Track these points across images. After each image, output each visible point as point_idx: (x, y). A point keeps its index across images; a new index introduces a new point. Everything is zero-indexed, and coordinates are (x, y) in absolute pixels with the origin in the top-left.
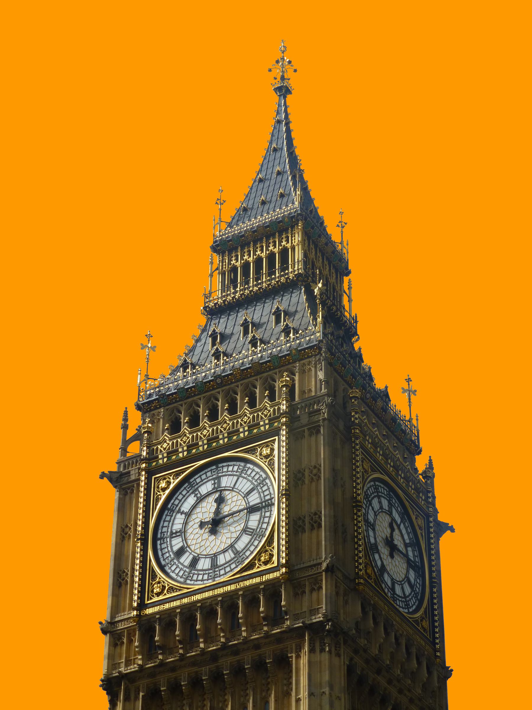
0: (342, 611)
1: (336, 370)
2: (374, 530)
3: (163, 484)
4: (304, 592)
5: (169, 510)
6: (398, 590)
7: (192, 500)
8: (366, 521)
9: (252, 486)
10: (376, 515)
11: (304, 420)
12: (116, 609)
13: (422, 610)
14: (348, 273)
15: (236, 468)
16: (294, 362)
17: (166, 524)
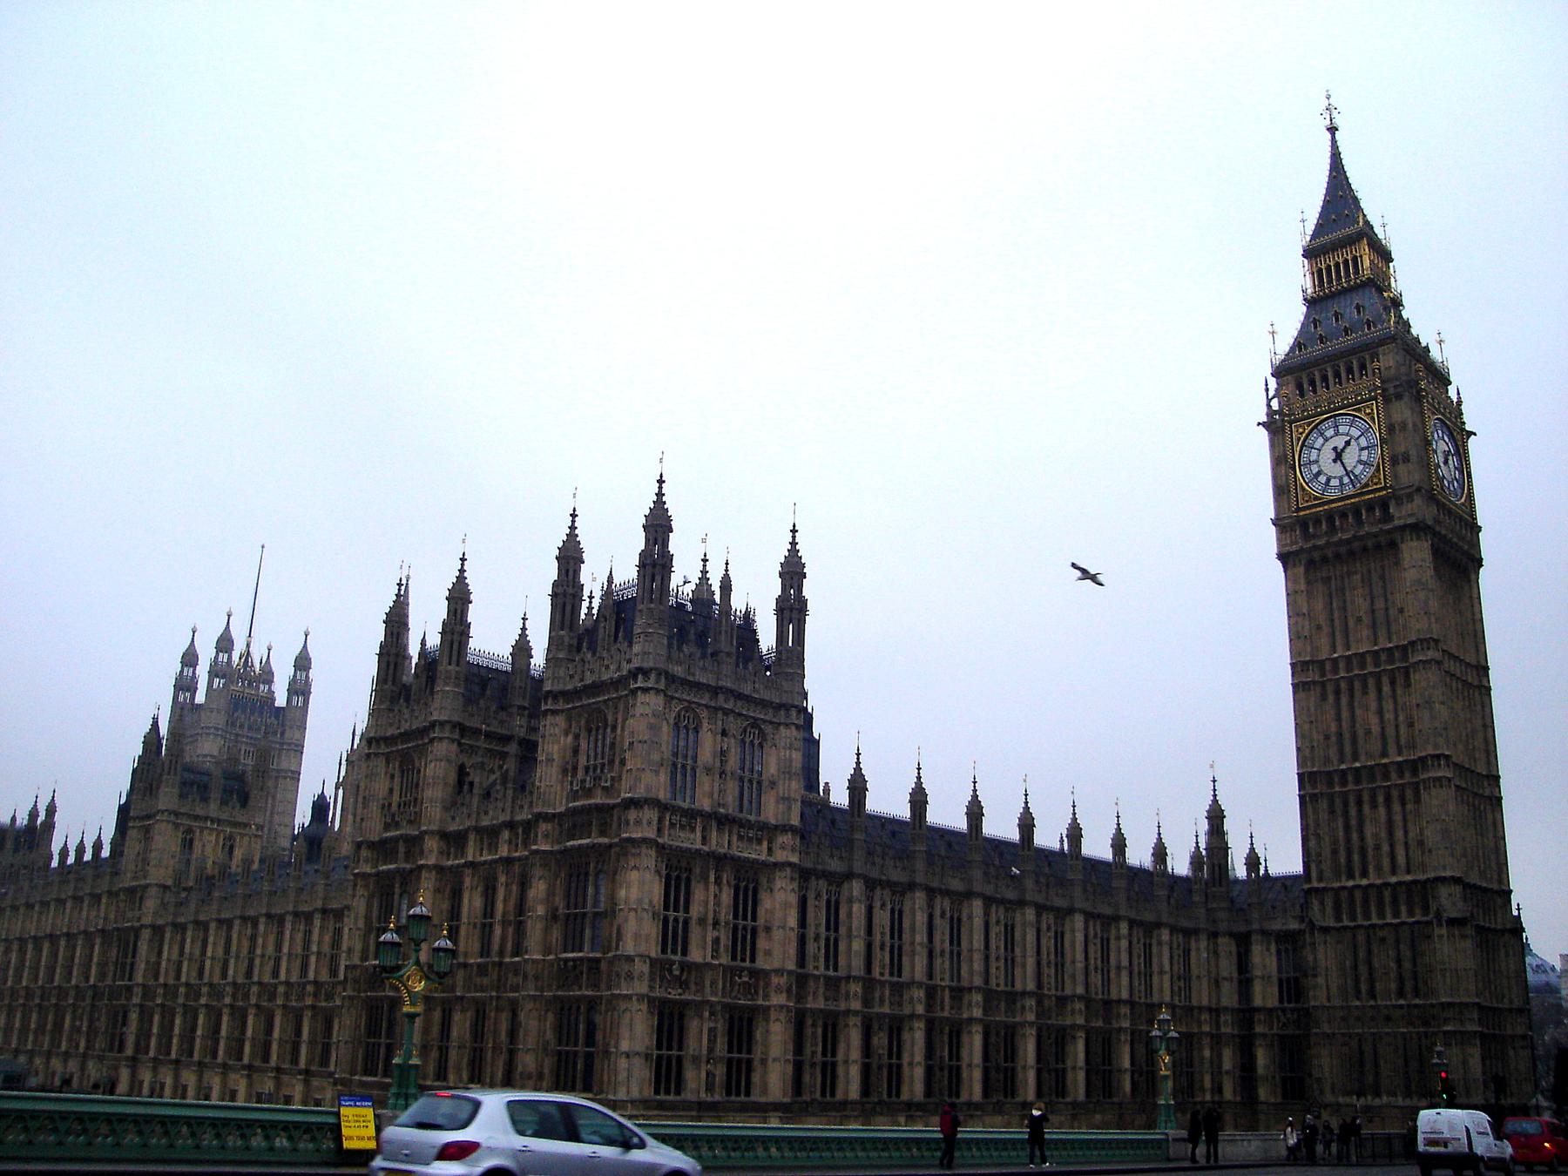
7: (1321, 440)
11: (1392, 391)
12: (1277, 513)
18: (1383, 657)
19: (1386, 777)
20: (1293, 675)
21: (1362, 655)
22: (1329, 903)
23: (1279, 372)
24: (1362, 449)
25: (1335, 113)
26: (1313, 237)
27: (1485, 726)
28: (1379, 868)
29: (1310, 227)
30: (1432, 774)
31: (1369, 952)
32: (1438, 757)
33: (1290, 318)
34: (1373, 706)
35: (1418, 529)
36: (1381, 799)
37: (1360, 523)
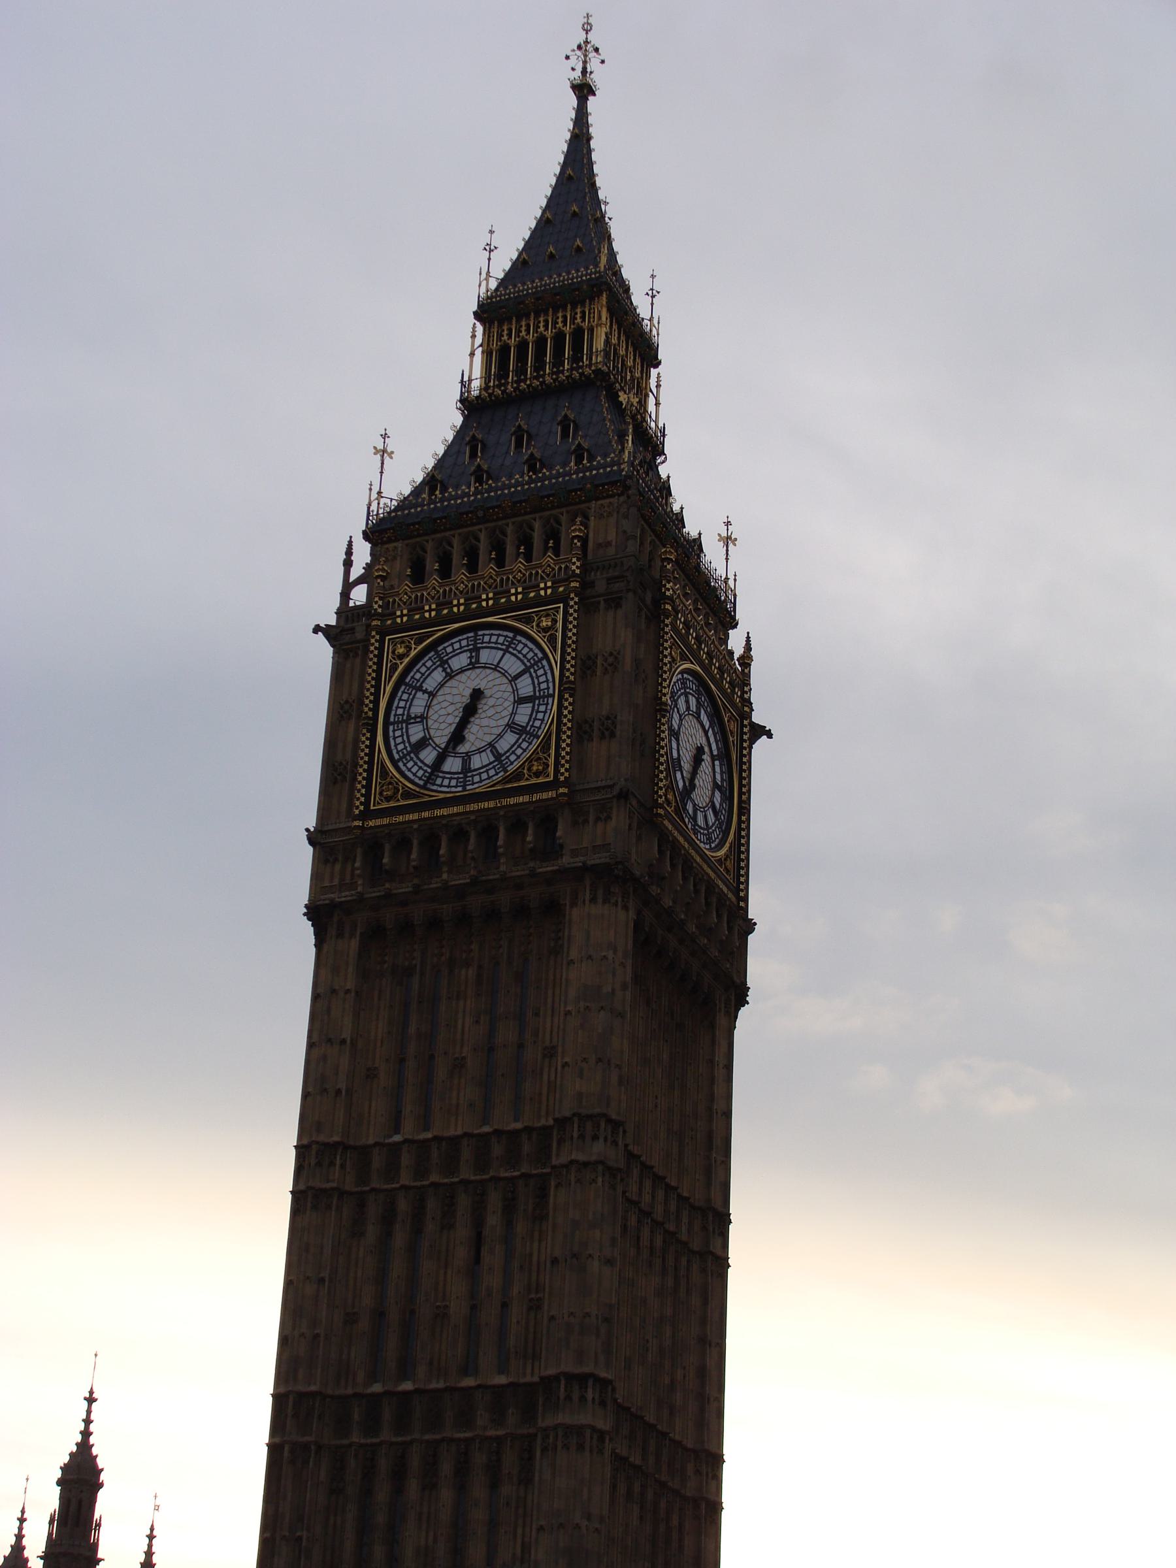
0: (634, 850)
1: (643, 516)
2: (677, 740)
3: (401, 650)
4: (586, 821)
5: (407, 685)
6: (700, 821)
7: (438, 675)
8: (670, 728)
9: (523, 667)
10: (681, 720)
11: (601, 586)
13: (727, 845)
14: (657, 364)
15: (501, 640)
16: (589, 500)
17: (402, 704)
18: (497, 1150)
21: (455, 1141)
24: (521, 701)
25: (594, 64)
26: (503, 283)
27: (703, 1341)
29: (502, 264)
30: (564, 1418)
32: (582, 1379)
33: (425, 431)
34: (461, 1254)
35: (609, 878)
36: (446, 1468)
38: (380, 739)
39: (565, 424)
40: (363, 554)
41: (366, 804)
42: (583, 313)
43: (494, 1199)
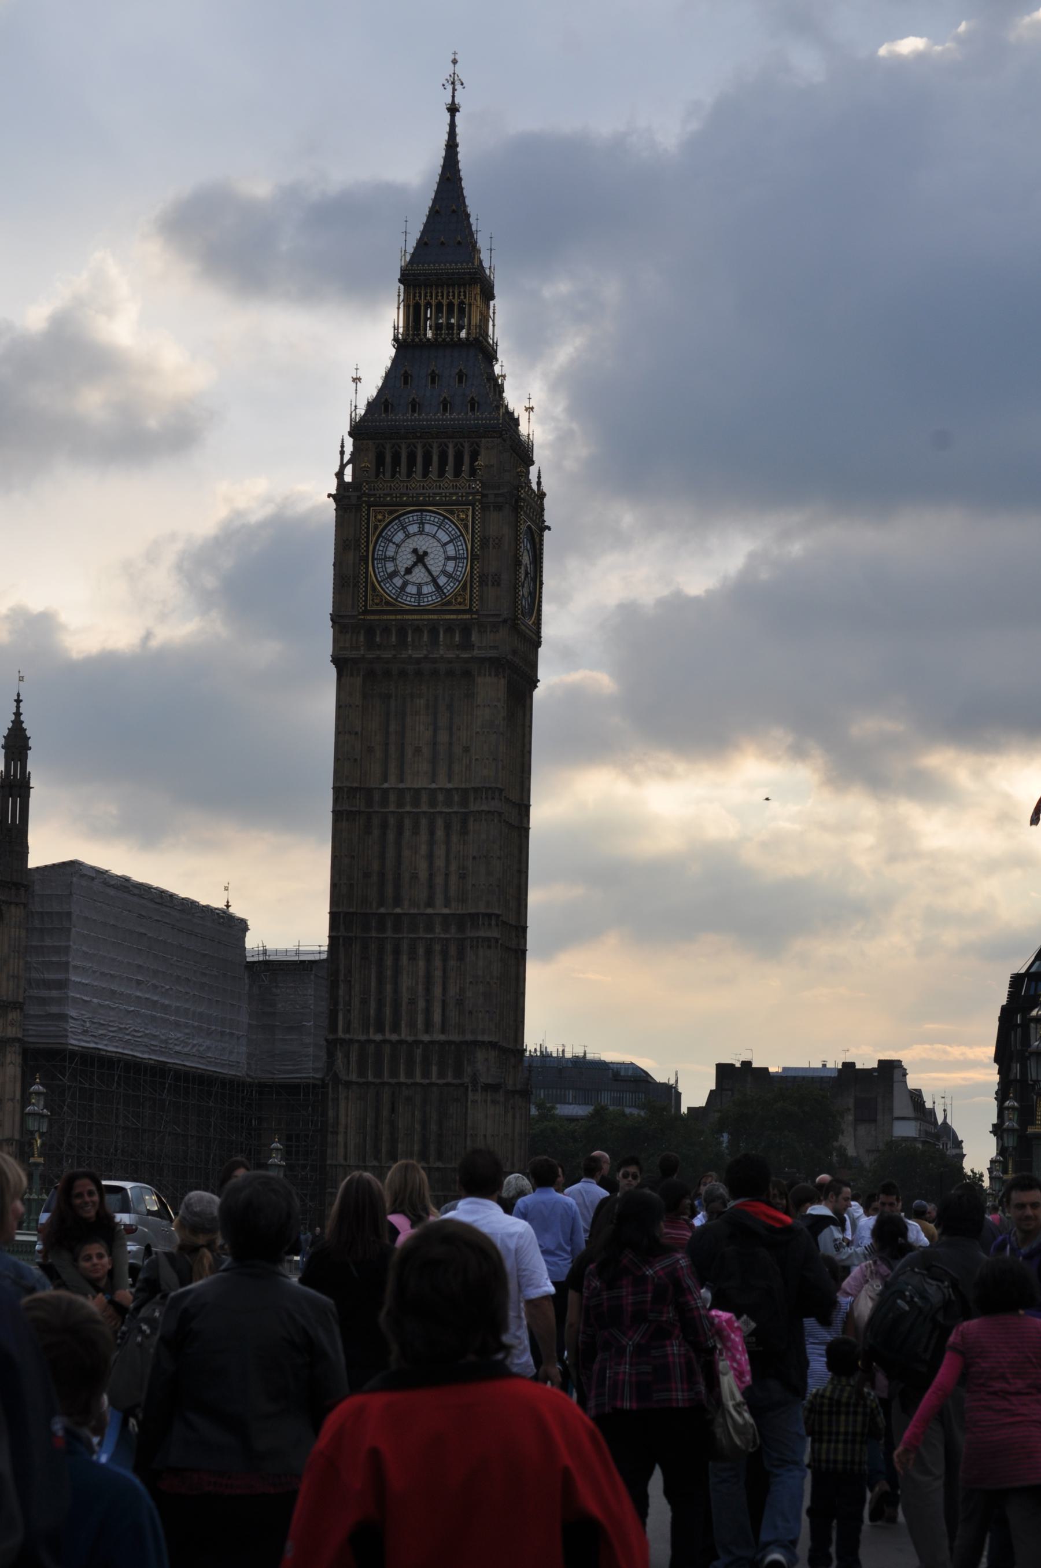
3: (380, 517)
7: (400, 535)
18: (441, 797)
19: (430, 928)
20: (336, 800)
21: (417, 791)
22: (354, 1057)
23: (357, 430)
24: (448, 558)
25: (458, 87)
28: (412, 1025)
30: (482, 934)
31: (393, 1110)
32: (489, 916)
34: (423, 849)
36: (421, 951)
37: (434, 641)
38: (370, 568)
39: (461, 376)
40: (349, 443)
41: (365, 606)
42: (465, 292)
43: (440, 822)
